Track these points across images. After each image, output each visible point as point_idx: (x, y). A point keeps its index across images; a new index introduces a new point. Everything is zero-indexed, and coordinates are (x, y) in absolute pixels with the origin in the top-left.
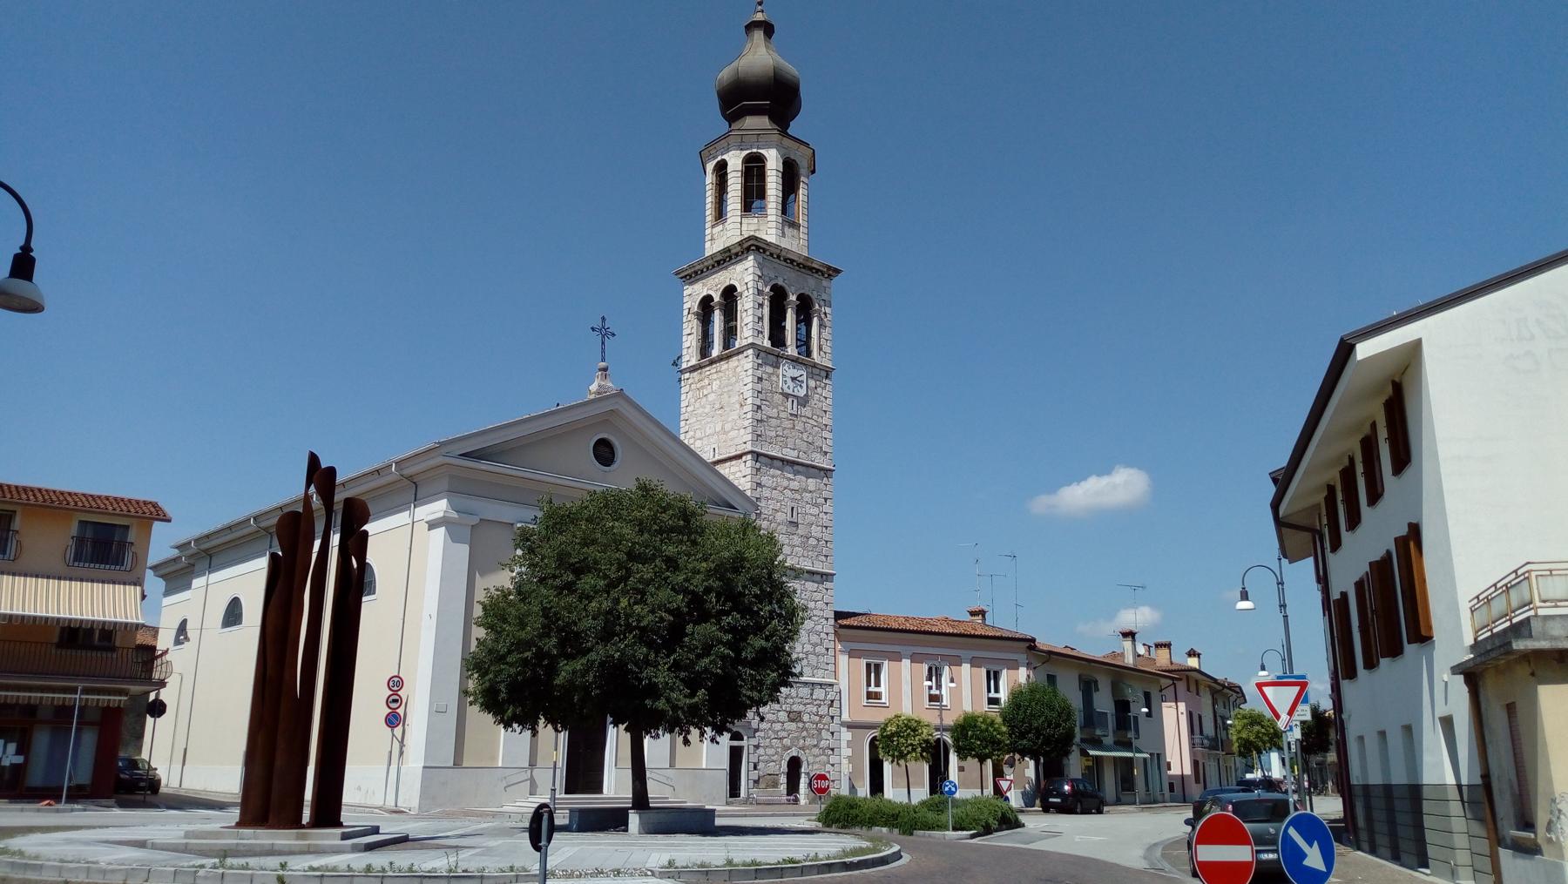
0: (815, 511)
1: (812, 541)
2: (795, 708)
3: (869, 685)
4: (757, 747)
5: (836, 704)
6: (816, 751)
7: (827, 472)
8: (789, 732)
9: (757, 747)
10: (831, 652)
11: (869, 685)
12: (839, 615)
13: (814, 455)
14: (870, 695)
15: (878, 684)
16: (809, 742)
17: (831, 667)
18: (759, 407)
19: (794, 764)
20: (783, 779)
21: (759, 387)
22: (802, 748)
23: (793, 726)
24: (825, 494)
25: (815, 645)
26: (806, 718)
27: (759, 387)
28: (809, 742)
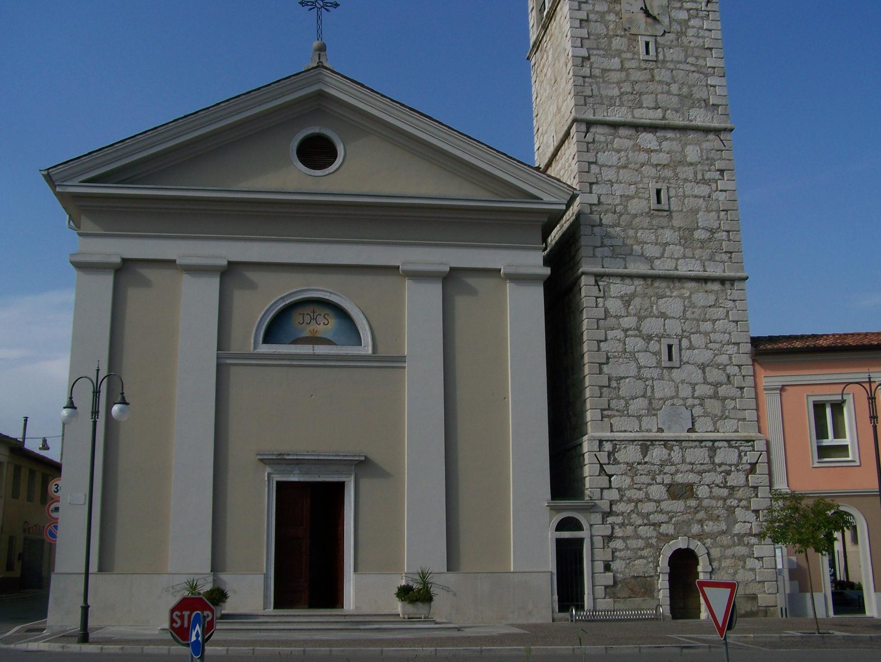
0: (703, 190)
1: (700, 234)
2: (679, 478)
3: (821, 433)
4: (610, 538)
5: (761, 468)
6: (725, 540)
7: (731, 130)
8: (671, 515)
9: (610, 538)
10: (748, 392)
11: (821, 433)
12: (756, 341)
13: (693, 112)
14: (824, 452)
15: (839, 432)
16: (709, 527)
17: (751, 415)
18: (585, 59)
19: (683, 564)
20: (663, 584)
21: (584, 33)
22: (700, 537)
23: (678, 505)
24: (719, 165)
25: (717, 385)
26: (702, 491)
27: (584, 33)
28: (709, 527)
